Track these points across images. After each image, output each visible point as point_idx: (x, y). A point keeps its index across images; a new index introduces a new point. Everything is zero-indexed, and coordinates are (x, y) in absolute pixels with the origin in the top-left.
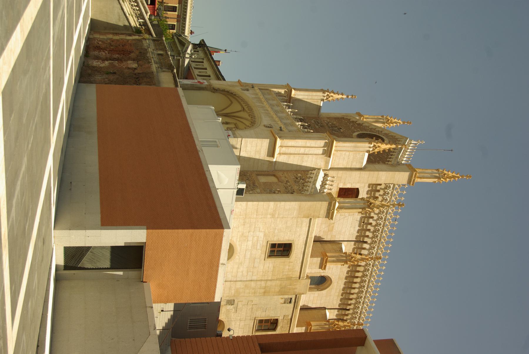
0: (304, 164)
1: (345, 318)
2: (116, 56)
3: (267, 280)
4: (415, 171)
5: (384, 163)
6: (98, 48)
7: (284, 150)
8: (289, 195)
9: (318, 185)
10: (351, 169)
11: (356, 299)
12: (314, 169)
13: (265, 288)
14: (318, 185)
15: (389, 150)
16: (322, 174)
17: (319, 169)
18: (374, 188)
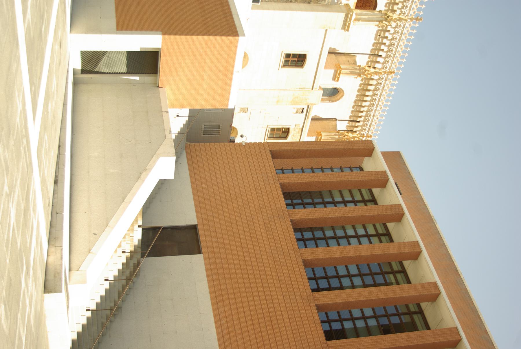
1: (355, 130)
3: (280, 90)
11: (367, 111)
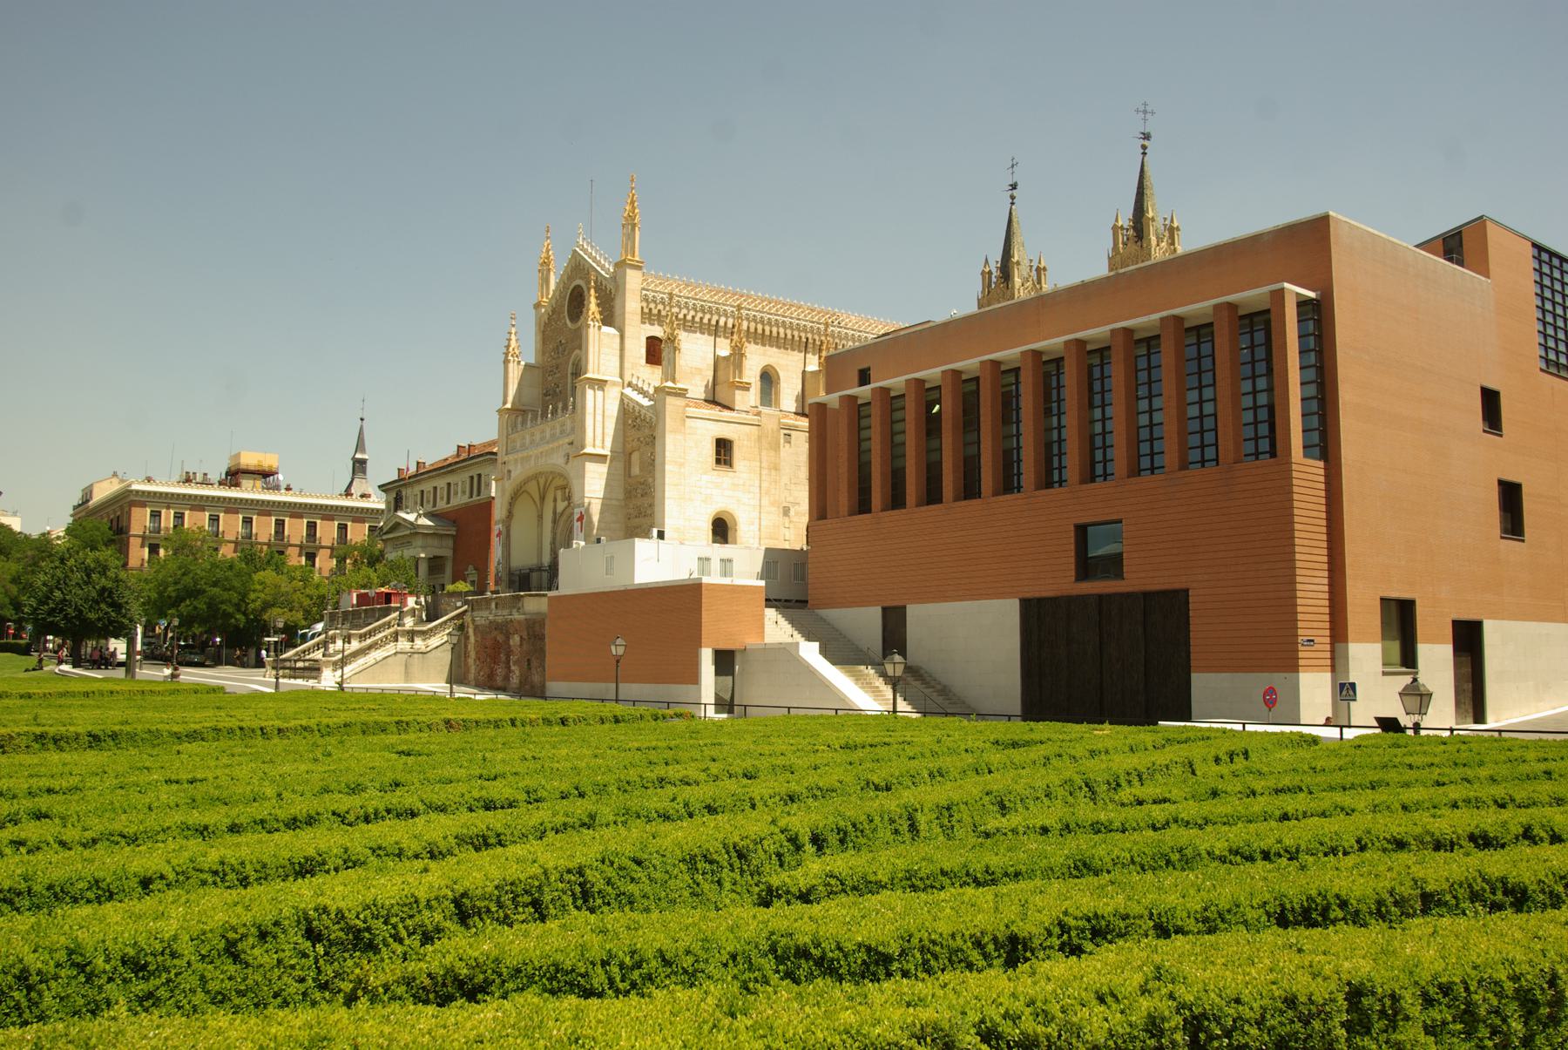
0: (615, 414)
1: (818, 343)
2: (503, 656)
4: (625, 260)
5: (613, 299)
6: (491, 676)
7: (599, 442)
8: (657, 442)
9: (646, 402)
10: (622, 349)
11: (792, 329)
12: (622, 400)
13: (770, 469)
14: (646, 402)
15: (597, 298)
16: (629, 392)
17: (622, 393)
18: (648, 317)
